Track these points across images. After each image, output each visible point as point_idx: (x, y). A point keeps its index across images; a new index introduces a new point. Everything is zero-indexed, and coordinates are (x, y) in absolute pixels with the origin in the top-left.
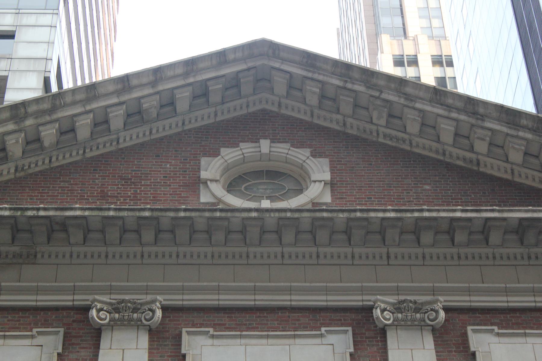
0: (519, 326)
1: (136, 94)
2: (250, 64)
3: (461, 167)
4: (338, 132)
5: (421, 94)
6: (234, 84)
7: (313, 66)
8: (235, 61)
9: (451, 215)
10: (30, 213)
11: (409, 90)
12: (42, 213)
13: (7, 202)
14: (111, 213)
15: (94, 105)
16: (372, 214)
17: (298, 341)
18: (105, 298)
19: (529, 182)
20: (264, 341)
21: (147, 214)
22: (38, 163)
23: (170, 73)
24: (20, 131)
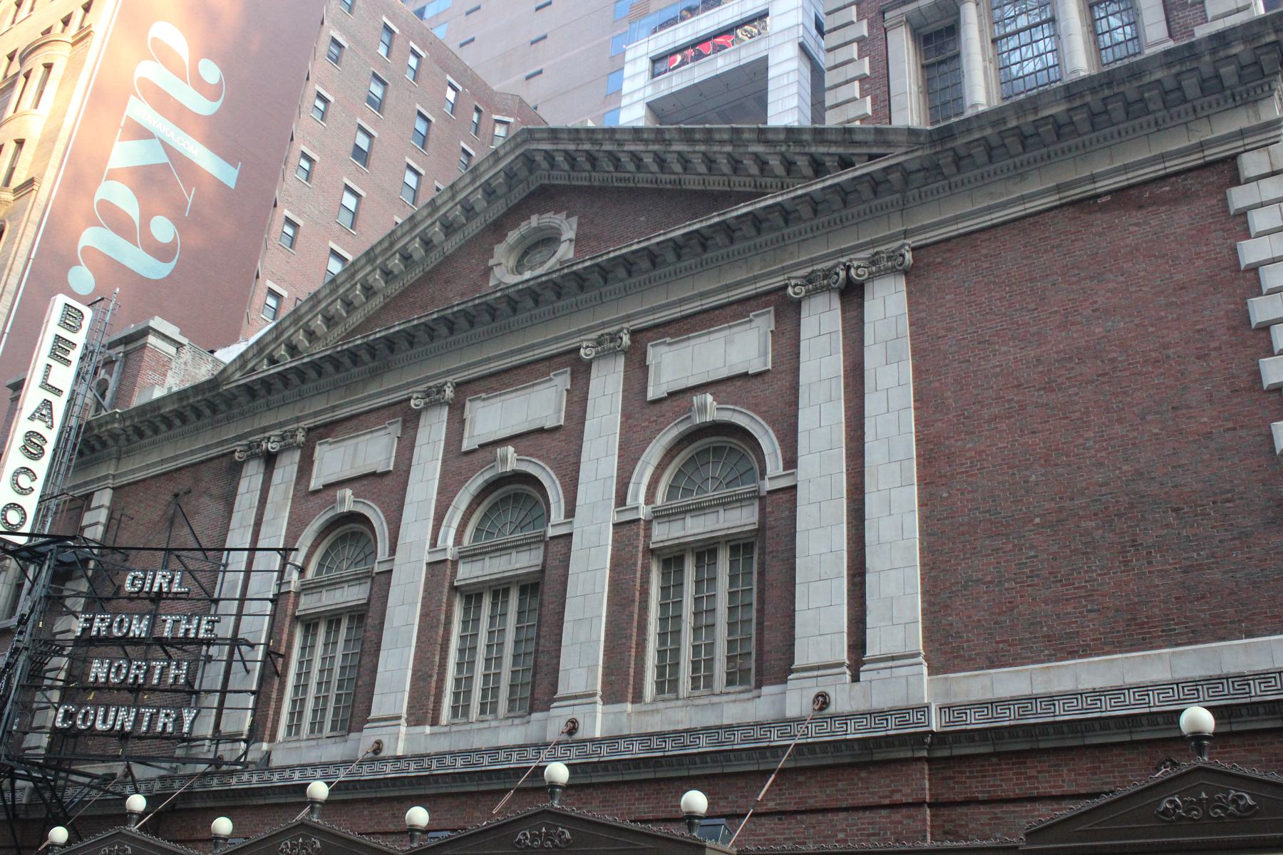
0: (688, 331)
1: (442, 211)
2: (518, 152)
3: (668, 190)
4: (589, 187)
5: (626, 137)
6: (510, 174)
7: (556, 138)
8: (506, 154)
9: (629, 249)
10: (372, 338)
11: (618, 136)
12: (378, 335)
13: (377, 326)
14: (415, 322)
15: (417, 231)
16: (575, 268)
17: (536, 388)
18: (419, 388)
19: (717, 188)
20: (514, 395)
21: (435, 316)
22: (396, 288)
23: (461, 185)
24: (374, 270)
